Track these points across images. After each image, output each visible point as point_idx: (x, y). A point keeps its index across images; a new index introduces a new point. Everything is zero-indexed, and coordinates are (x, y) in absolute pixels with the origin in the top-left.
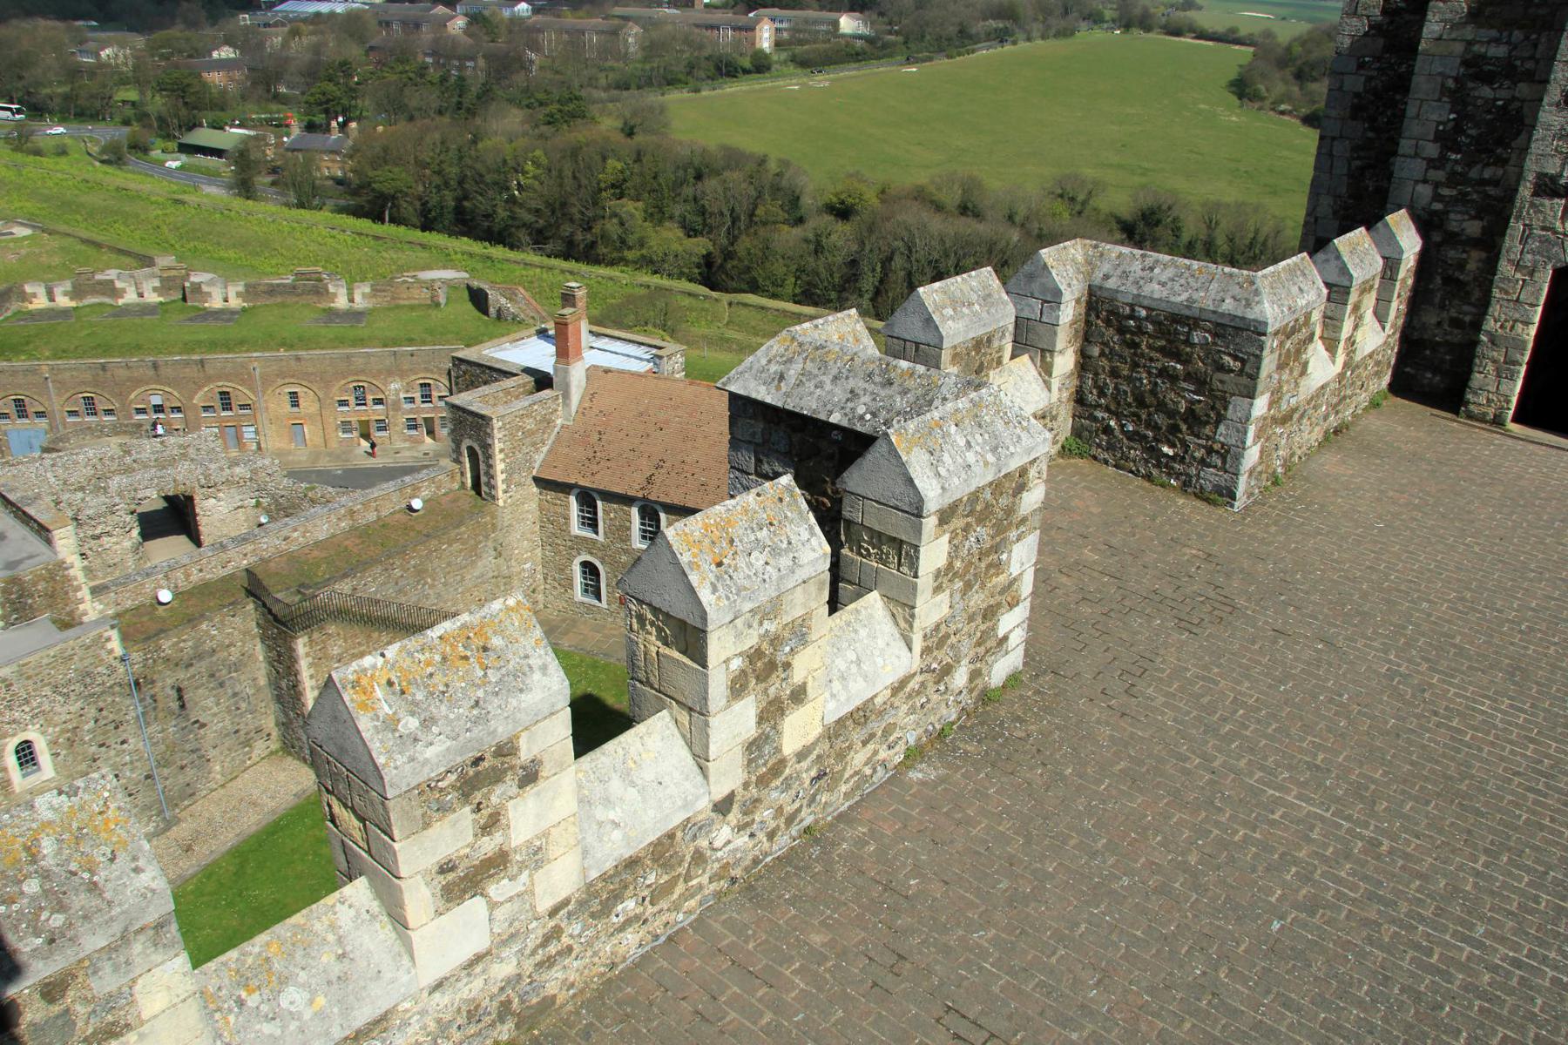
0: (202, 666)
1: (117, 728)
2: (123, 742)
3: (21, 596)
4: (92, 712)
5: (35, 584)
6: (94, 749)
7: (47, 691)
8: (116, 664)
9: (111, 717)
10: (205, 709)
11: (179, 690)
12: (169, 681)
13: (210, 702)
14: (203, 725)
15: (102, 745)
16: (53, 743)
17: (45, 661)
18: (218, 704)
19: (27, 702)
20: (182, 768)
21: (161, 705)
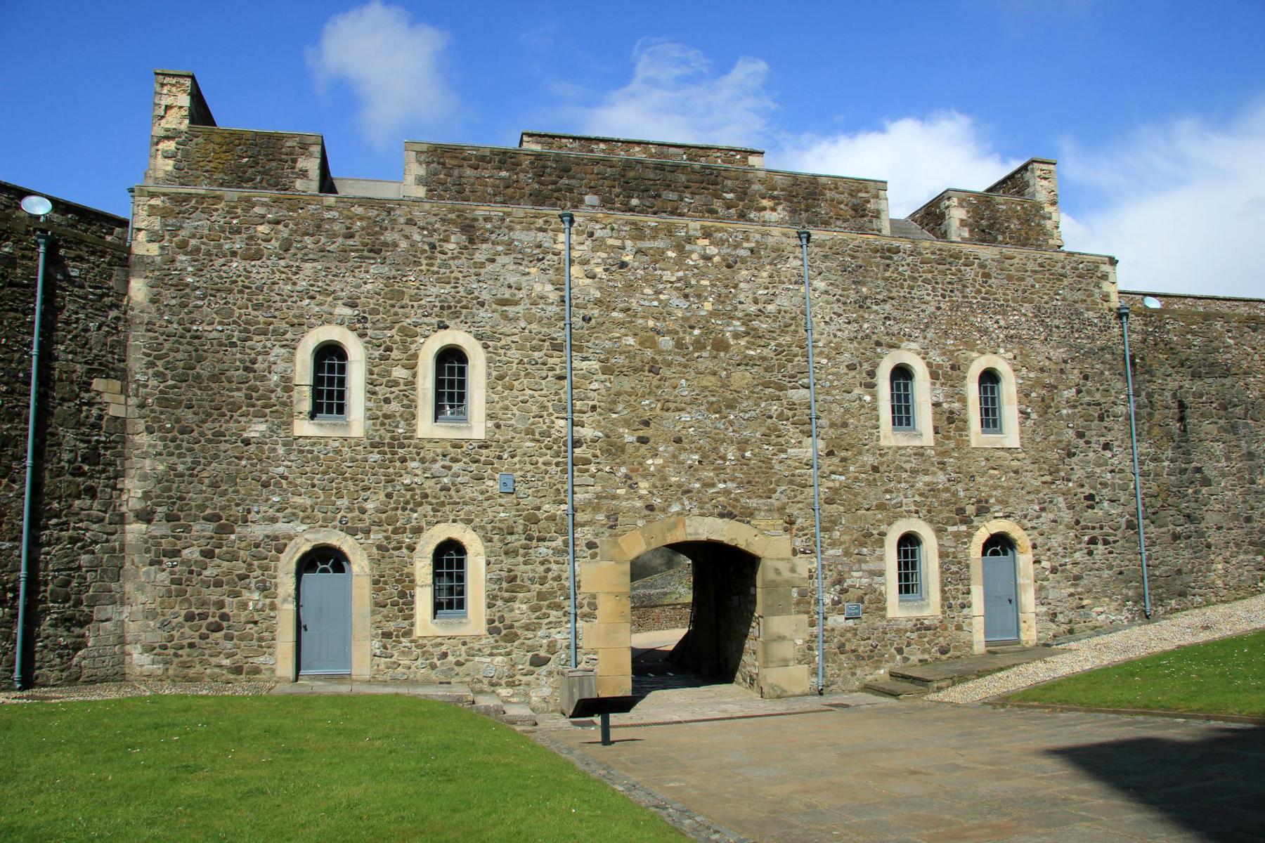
0: (1211, 385)
1: (1101, 418)
2: (1106, 446)
3: (991, 226)
4: (1075, 376)
5: (1008, 219)
6: (1070, 434)
7: (1027, 308)
8: (1111, 317)
9: (1098, 396)
10: (1212, 456)
11: (1182, 406)
12: (1172, 384)
13: (1218, 448)
14: (1206, 482)
15: (1080, 435)
16: (1024, 394)
17: (1031, 266)
18: (1228, 459)
19: (1004, 313)
20: (1176, 537)
21: (1157, 416)
